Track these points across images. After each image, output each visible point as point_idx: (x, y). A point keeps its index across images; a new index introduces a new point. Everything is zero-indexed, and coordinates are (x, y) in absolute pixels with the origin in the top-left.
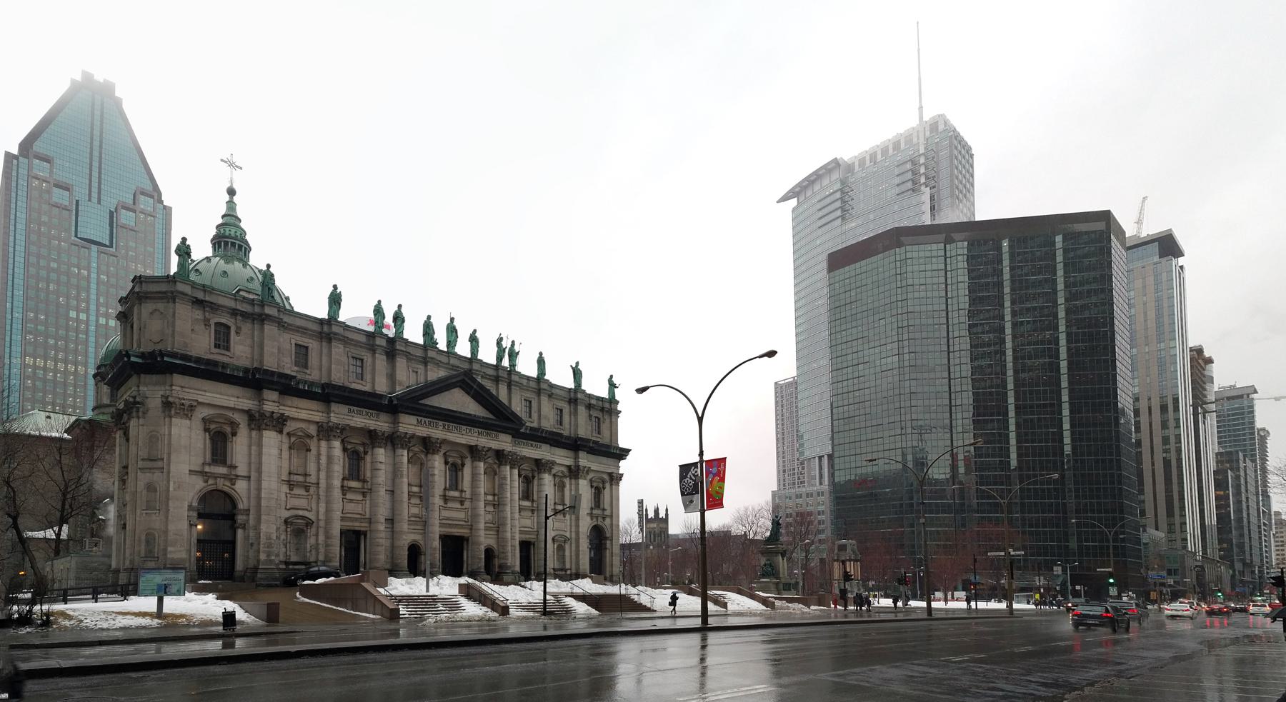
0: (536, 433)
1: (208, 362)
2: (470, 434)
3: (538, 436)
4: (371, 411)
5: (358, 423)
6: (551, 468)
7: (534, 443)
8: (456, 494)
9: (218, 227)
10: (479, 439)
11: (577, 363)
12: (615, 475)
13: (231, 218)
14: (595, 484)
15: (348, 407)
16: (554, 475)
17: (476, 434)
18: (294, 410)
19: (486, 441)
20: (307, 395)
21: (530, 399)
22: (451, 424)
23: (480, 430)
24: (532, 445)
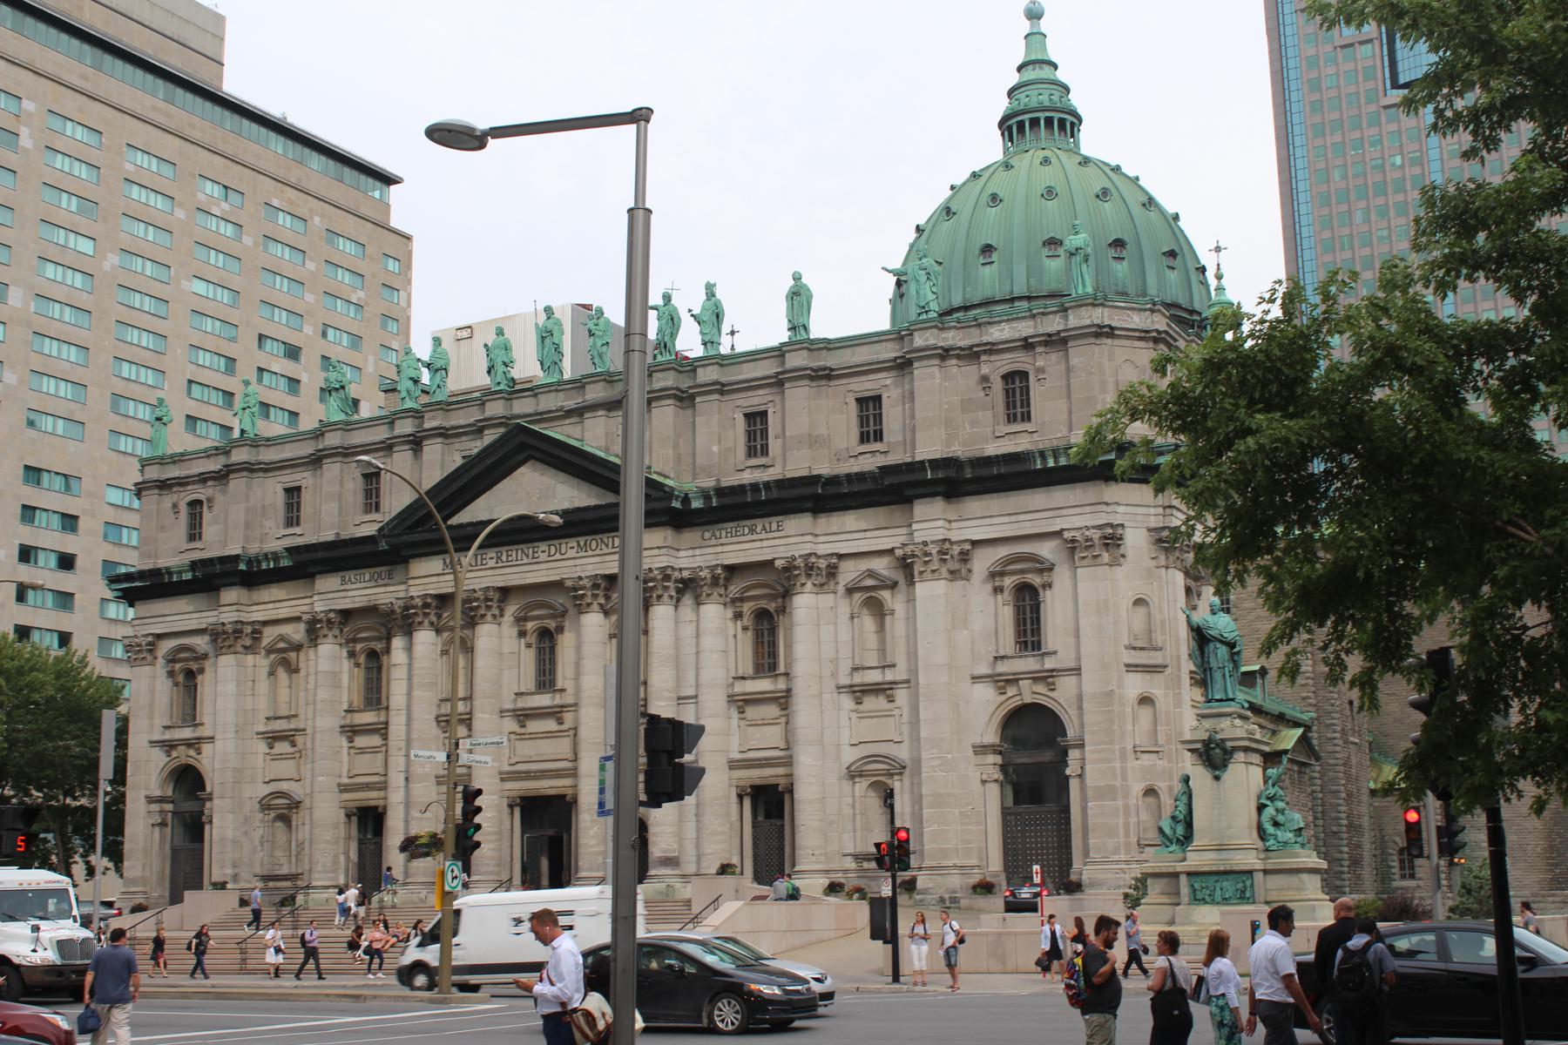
0: (738, 499)
1: (142, 575)
2: (558, 556)
4: (378, 569)
5: (357, 599)
6: (832, 572)
8: (544, 700)
9: (1011, 93)
10: (578, 562)
12: (1067, 535)
13: (1036, 63)
14: (1008, 582)
17: (572, 553)
18: (271, 606)
20: (278, 576)
21: (762, 408)
22: (516, 547)
23: (582, 540)
24: (752, 531)
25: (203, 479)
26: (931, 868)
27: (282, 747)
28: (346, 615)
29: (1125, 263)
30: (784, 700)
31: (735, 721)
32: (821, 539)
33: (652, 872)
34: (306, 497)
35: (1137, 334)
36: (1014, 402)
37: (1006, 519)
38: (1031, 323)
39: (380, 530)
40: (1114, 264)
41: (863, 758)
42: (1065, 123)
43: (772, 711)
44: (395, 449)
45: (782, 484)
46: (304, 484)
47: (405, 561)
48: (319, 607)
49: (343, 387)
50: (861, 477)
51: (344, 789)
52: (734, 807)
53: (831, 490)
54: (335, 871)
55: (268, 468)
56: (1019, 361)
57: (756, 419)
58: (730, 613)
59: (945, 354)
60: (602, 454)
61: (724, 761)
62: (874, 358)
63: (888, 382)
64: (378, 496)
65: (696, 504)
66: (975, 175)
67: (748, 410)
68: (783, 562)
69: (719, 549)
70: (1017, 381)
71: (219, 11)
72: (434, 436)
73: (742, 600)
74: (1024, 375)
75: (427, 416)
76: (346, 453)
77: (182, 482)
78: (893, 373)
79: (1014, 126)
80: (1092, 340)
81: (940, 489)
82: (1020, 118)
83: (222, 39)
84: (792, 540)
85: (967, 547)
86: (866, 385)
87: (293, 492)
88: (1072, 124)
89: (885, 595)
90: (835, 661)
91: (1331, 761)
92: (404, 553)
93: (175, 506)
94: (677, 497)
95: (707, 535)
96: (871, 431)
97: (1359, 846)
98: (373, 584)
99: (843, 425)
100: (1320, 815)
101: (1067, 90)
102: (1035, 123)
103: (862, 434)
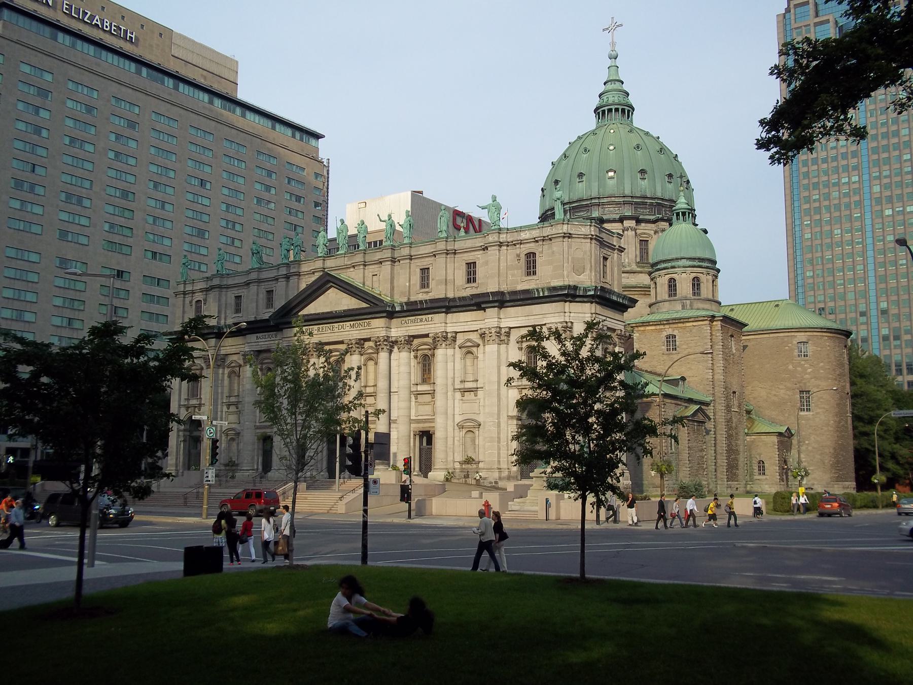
2: (342, 330)
3: (414, 309)
4: (271, 333)
6: (454, 339)
7: (424, 317)
9: (600, 96)
11: (494, 199)
12: (548, 326)
14: (524, 345)
15: (257, 335)
16: (460, 348)
17: (348, 329)
19: (357, 332)
21: (427, 267)
23: (352, 323)
24: (421, 320)
25: (202, 290)
26: (487, 469)
27: (233, 409)
28: (259, 352)
29: (646, 181)
30: (432, 393)
31: (413, 403)
32: (448, 325)
33: (376, 468)
34: (244, 300)
35: (583, 236)
36: (530, 266)
37: (524, 318)
38: (538, 231)
39: (270, 317)
40: (640, 180)
41: (463, 420)
42: (627, 111)
43: (427, 398)
44: (279, 280)
45: (432, 301)
46: (242, 294)
47: (281, 330)
48: (247, 349)
49: (259, 252)
50: (464, 298)
51: (257, 428)
52: (412, 440)
53: (452, 304)
54: (253, 463)
55: (228, 287)
56: (530, 247)
57: (425, 271)
58: (412, 357)
59: (501, 245)
60: (360, 286)
61: (407, 420)
62: (474, 245)
63: (479, 256)
64: (272, 301)
65: (398, 309)
66: (579, 138)
67: (422, 267)
68: (433, 335)
69: (408, 328)
70: (532, 255)
71: (236, 59)
72: (295, 275)
73: (417, 350)
74: (534, 254)
75: (292, 266)
76: (259, 281)
77: (193, 292)
78: (481, 252)
79: (601, 112)
80: (561, 239)
81: (496, 304)
82: (603, 109)
83: (237, 72)
84: (437, 325)
85: (507, 330)
86: (470, 257)
87: (238, 298)
88: (629, 111)
89: (474, 349)
90: (454, 378)
91: (720, 420)
92: (280, 327)
93: (191, 302)
94: (389, 306)
95: (403, 322)
96: (471, 277)
97: (736, 459)
98: (269, 339)
99: (461, 275)
100: (713, 445)
101: (628, 94)
102: (610, 110)
103: (468, 279)
